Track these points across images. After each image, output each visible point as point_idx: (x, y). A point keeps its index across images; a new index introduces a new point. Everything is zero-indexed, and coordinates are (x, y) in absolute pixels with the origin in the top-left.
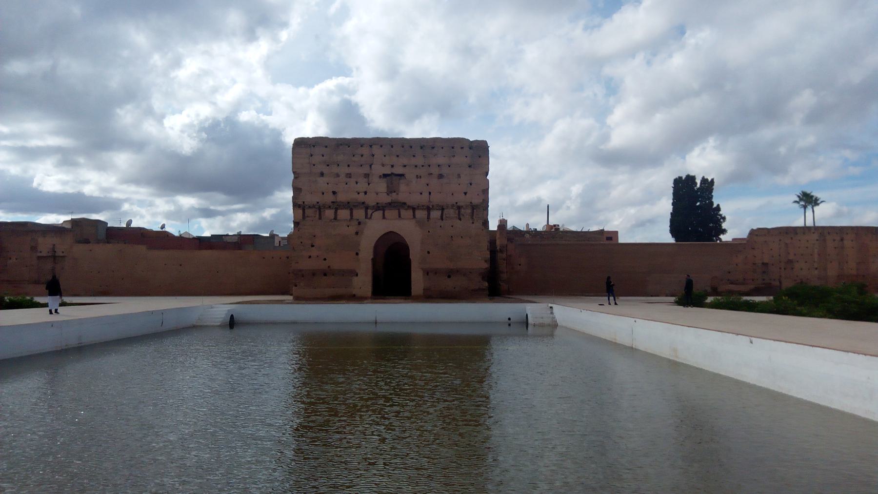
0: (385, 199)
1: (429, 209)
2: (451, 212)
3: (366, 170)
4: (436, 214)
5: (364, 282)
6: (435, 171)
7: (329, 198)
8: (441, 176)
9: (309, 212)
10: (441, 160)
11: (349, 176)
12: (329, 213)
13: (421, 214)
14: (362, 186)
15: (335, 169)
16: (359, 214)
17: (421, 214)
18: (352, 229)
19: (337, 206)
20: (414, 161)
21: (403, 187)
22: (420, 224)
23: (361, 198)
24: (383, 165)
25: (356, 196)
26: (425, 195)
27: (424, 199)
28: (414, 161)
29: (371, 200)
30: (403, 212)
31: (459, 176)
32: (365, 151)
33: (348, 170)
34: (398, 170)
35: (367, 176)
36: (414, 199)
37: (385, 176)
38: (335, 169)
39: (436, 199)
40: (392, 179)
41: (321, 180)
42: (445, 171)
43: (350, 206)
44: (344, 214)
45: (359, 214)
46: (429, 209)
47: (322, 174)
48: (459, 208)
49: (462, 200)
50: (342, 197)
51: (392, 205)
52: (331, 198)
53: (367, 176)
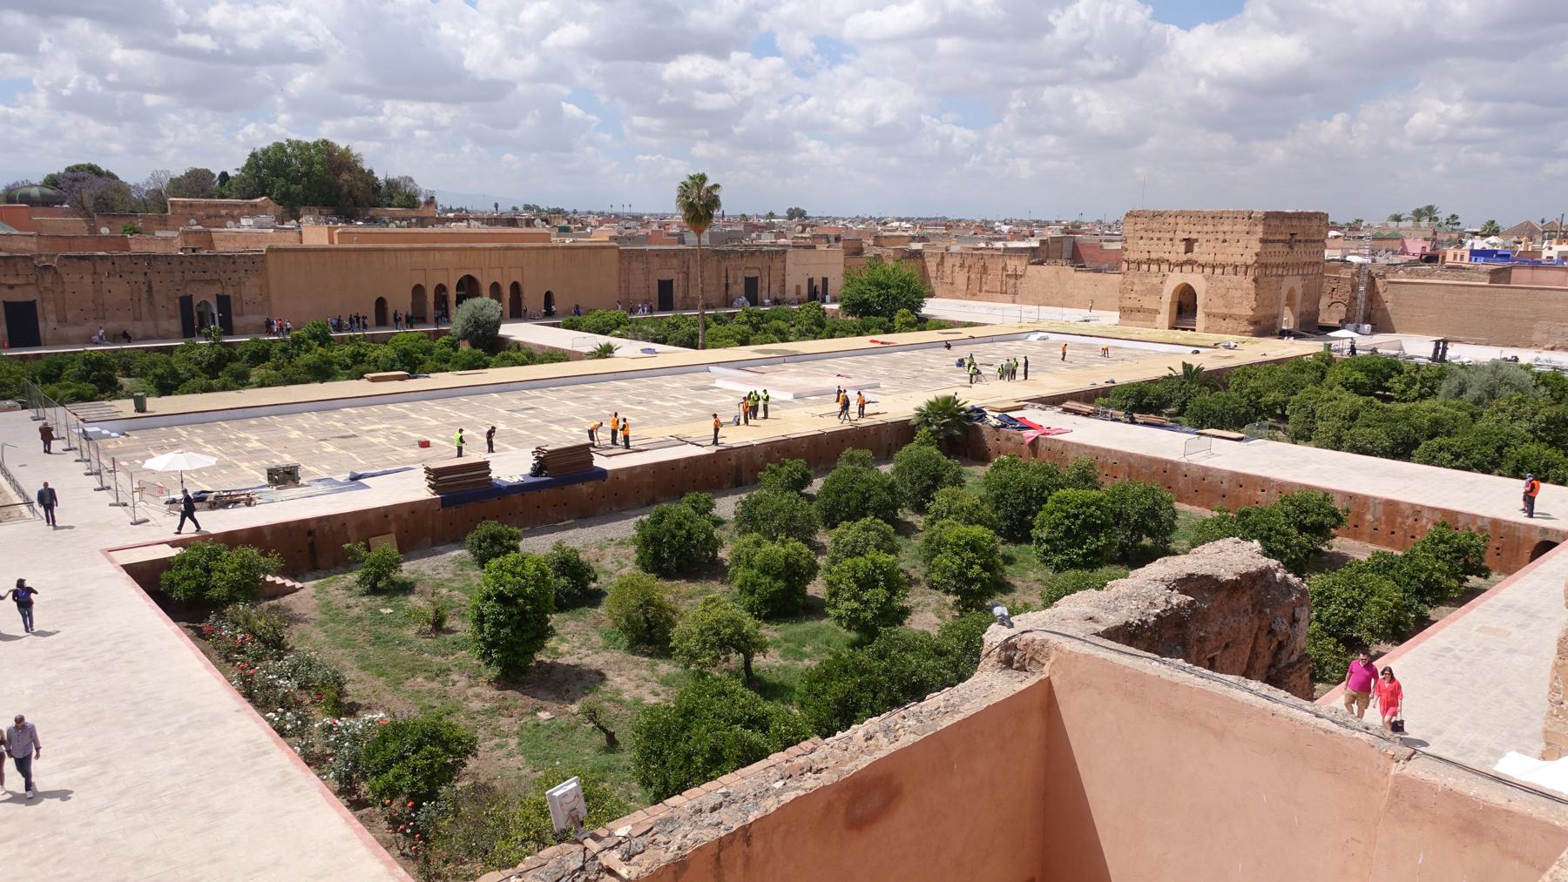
0: (1184, 258)
1: (1213, 267)
2: (1230, 269)
3: (1171, 235)
4: (1218, 271)
5: (1164, 317)
6: (1221, 237)
7: (1146, 256)
8: (1225, 241)
9: (1132, 266)
10: (1225, 229)
11: (1159, 239)
12: (1145, 267)
13: (1208, 270)
14: (1168, 247)
15: (1151, 235)
16: (1165, 267)
17: (1208, 270)
18: (1159, 280)
19: (1149, 261)
20: (1205, 229)
21: (1196, 249)
22: (1207, 279)
23: (1166, 256)
24: (1183, 231)
25: (1162, 255)
26: (1212, 255)
27: (1210, 259)
28: (1205, 229)
29: (1172, 258)
30: (1195, 267)
31: (1238, 241)
32: (1172, 220)
33: (1158, 235)
34: (1193, 236)
35: (1171, 240)
36: (1202, 259)
37: (1185, 240)
38: (1151, 235)
39: (1220, 259)
40: (1189, 244)
41: (1141, 242)
42: (1228, 237)
43: (1159, 262)
44: (1154, 268)
45: (1165, 267)
46: (1213, 267)
47: (1142, 238)
48: (1236, 266)
49: (1239, 260)
50: (1154, 256)
51: (1188, 262)
52: (1147, 256)
53: (1171, 240)
